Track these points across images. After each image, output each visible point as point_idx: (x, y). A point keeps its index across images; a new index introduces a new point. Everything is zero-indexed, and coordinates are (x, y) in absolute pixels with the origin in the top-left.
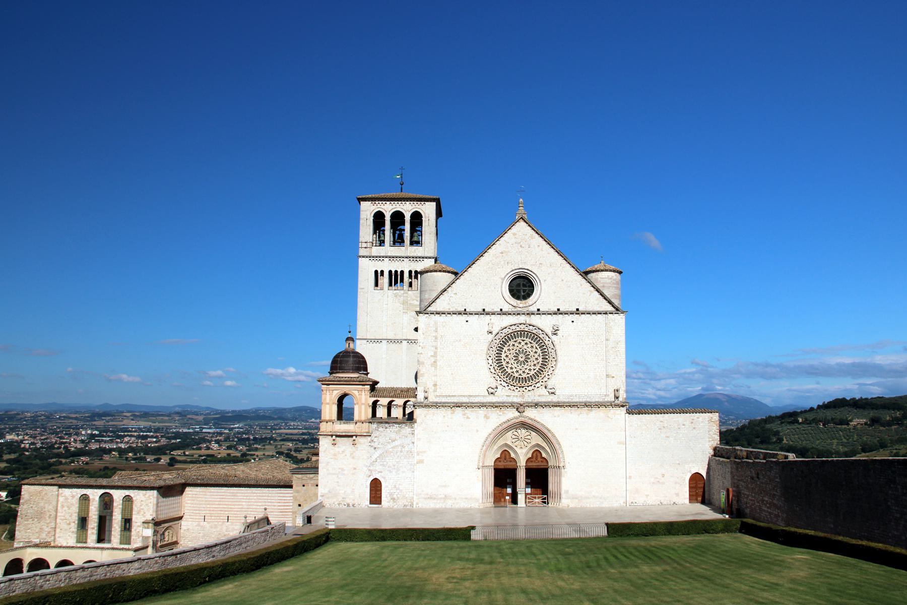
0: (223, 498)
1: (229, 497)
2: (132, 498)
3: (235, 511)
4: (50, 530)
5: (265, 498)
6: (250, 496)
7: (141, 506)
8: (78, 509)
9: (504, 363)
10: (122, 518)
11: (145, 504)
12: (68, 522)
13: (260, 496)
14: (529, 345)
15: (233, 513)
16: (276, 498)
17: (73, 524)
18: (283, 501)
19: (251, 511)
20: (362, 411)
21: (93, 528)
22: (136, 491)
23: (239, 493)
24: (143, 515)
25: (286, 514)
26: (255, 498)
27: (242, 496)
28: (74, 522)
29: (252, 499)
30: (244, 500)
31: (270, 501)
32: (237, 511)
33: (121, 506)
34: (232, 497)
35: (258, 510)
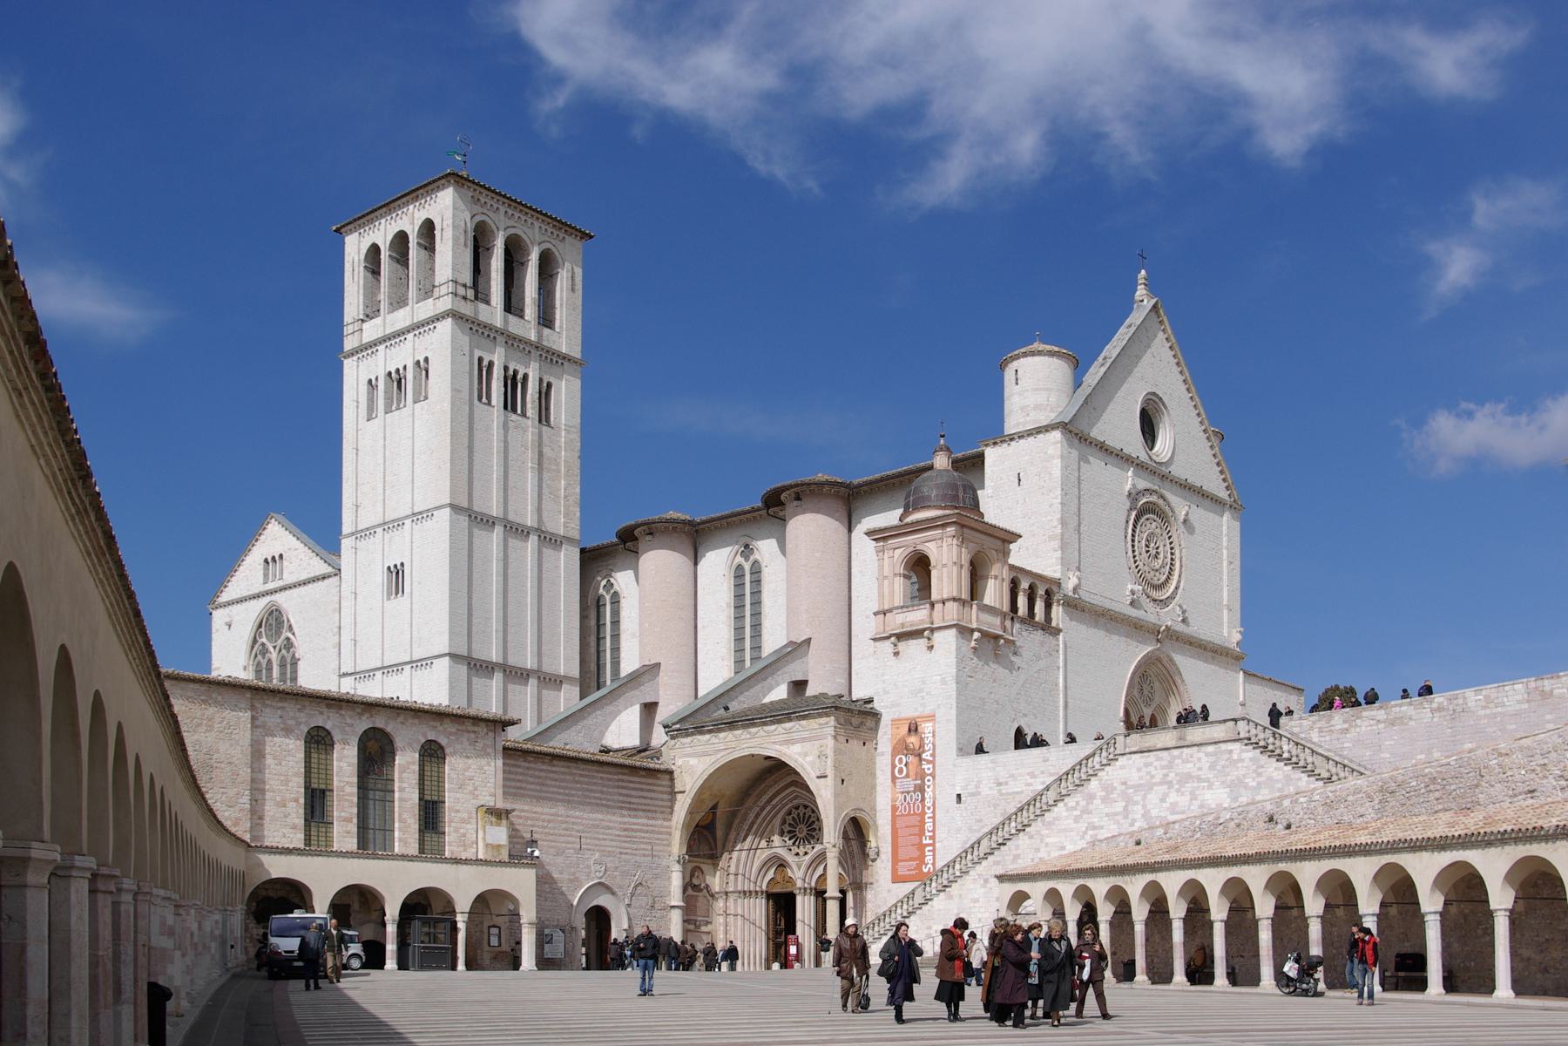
0: (521, 788)
1: (533, 787)
2: (442, 748)
3: (544, 821)
4: (237, 815)
5: (597, 795)
6: (571, 788)
7: (466, 770)
8: (303, 765)
9: (1136, 553)
10: (420, 799)
11: (474, 766)
12: (278, 799)
13: (588, 790)
14: (1158, 530)
15: (541, 823)
16: (616, 797)
17: (295, 804)
18: (627, 805)
19: (573, 823)
20: (994, 593)
21: (349, 820)
22: (450, 727)
23: (552, 779)
24: (471, 793)
25: (634, 834)
26: (580, 793)
27: (555, 786)
28: (296, 800)
29: (573, 796)
30: (561, 797)
31: (604, 802)
32: (549, 821)
33: (416, 768)
34: (538, 788)
35: (584, 821)
